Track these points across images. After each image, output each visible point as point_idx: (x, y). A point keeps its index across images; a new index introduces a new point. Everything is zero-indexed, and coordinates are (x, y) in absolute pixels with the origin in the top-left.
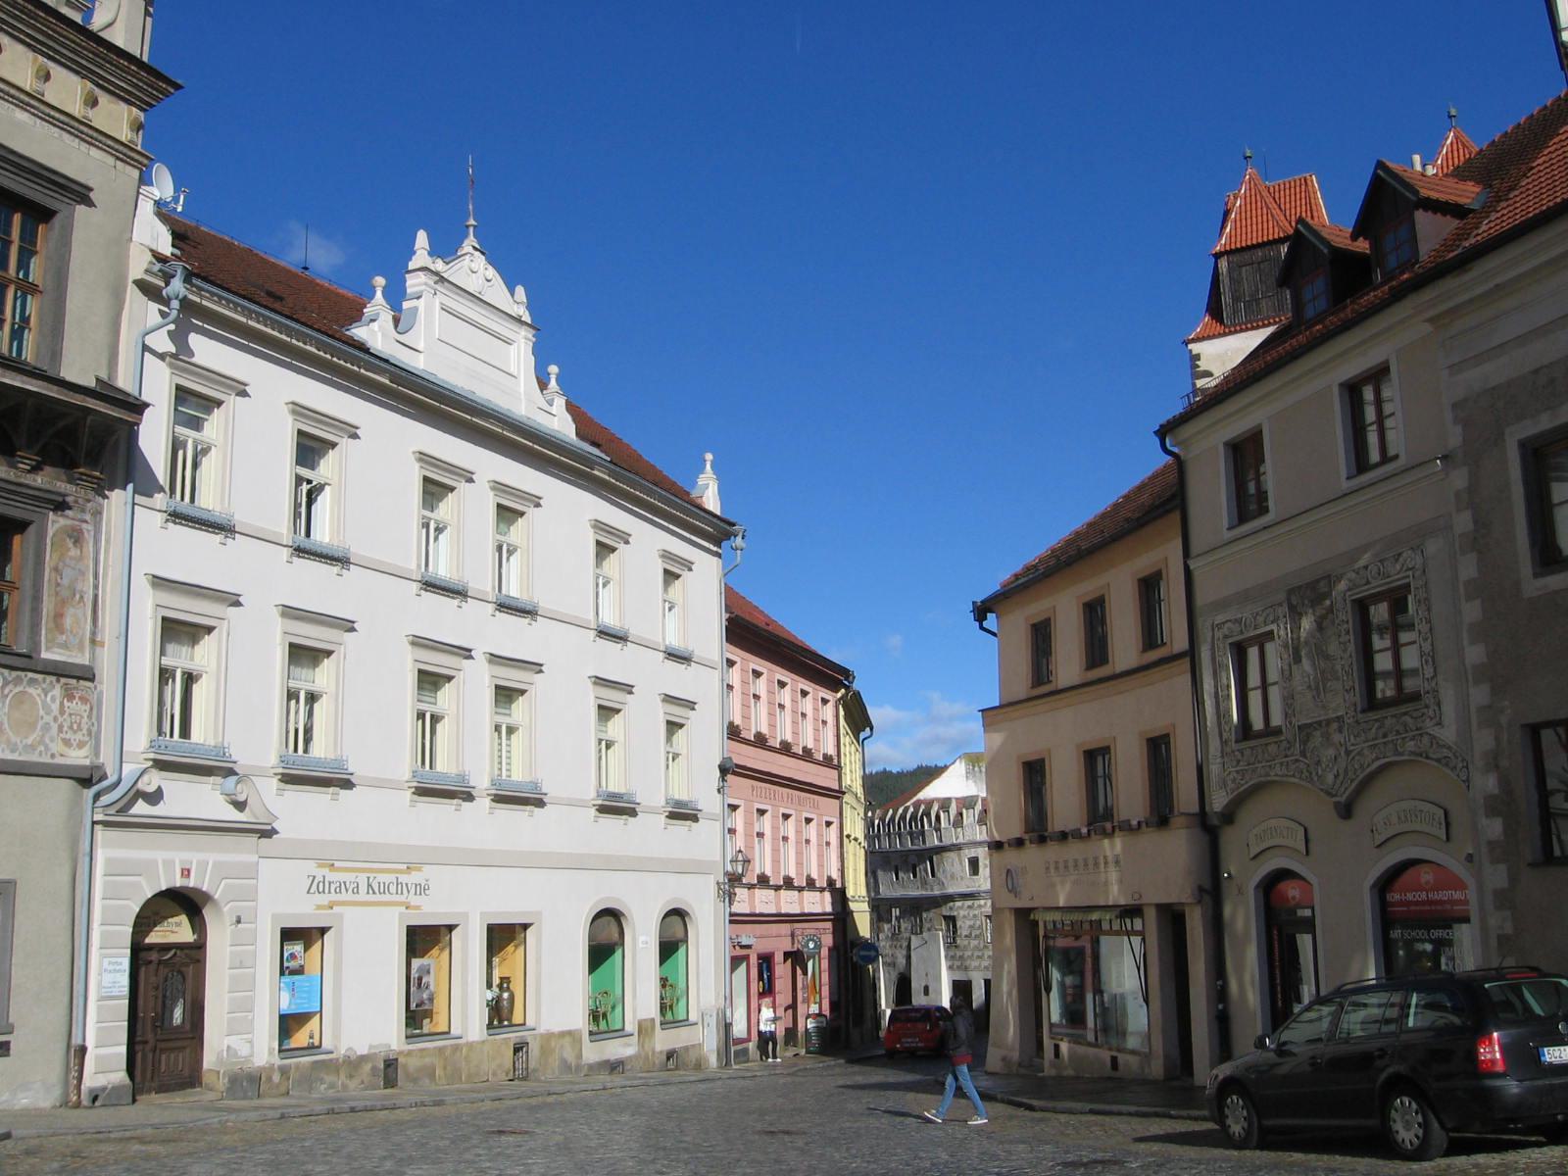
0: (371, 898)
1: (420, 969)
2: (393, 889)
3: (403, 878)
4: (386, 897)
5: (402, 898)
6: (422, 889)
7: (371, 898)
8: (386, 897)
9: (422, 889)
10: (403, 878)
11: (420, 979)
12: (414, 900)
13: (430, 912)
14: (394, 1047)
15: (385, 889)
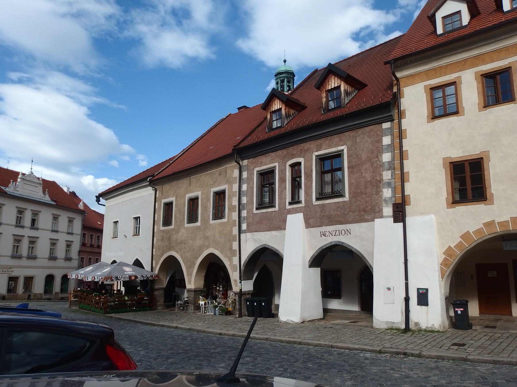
0: (2, 273)
1: (11, 283)
2: (7, 271)
3: (9, 270)
4: (5, 273)
5: (8, 273)
6: (12, 272)
7: (2, 273)
8: (5, 273)
9: (12, 272)
10: (9, 270)
11: (11, 285)
12: (10, 273)
13: (14, 274)
14: (5, 294)
15: (5, 271)
